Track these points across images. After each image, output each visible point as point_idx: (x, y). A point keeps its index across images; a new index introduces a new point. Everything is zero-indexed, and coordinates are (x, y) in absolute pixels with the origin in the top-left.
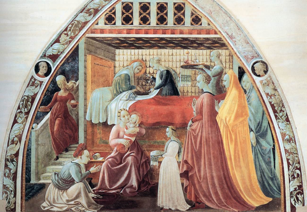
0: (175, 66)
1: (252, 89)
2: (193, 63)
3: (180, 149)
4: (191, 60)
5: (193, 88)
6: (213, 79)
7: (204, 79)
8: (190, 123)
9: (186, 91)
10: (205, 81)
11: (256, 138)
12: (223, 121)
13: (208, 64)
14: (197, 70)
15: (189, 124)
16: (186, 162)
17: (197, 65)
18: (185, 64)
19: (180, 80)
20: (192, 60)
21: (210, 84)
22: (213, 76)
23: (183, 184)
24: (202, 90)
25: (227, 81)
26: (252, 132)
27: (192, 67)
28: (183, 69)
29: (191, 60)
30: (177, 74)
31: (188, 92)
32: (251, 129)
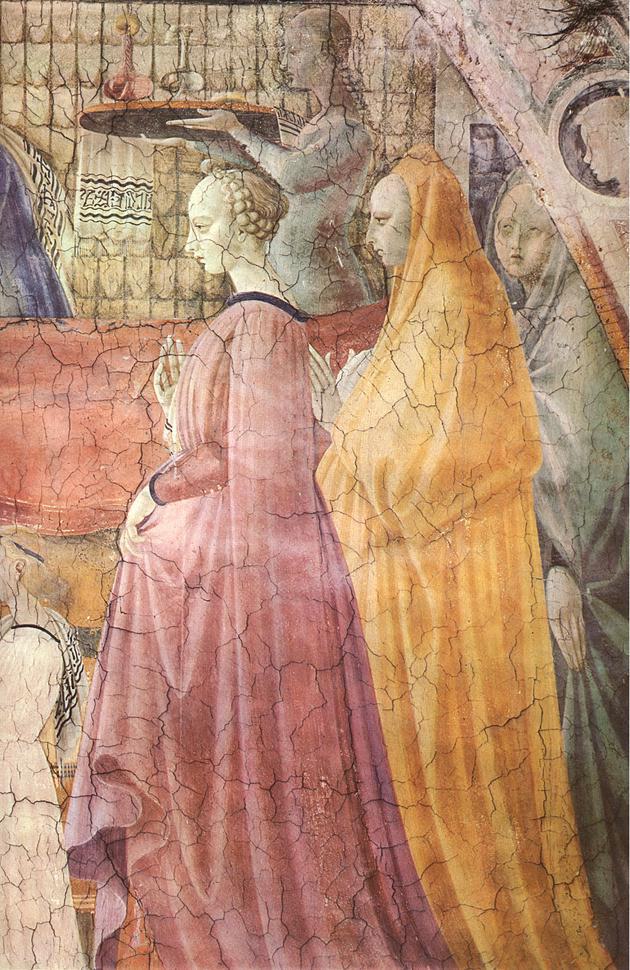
0: (39, 110)
1: (562, 282)
2: (161, 97)
3: (69, 682)
4: (152, 77)
5: (165, 272)
6: (294, 203)
7: (239, 206)
8: (141, 505)
9: (111, 290)
10: (241, 219)
11: (585, 609)
12: (364, 498)
13: (269, 99)
14: (191, 145)
15: (135, 513)
16: (107, 769)
17: (176, 114)
18: (108, 101)
19: (70, 213)
20: (160, 75)
21: (277, 246)
22: (300, 189)
23: (86, 922)
24: (225, 279)
25: (391, 222)
26: (557, 575)
27: (157, 120)
28: (97, 138)
29: (152, 77)
30: (54, 168)
31: (125, 290)
32: (554, 551)
